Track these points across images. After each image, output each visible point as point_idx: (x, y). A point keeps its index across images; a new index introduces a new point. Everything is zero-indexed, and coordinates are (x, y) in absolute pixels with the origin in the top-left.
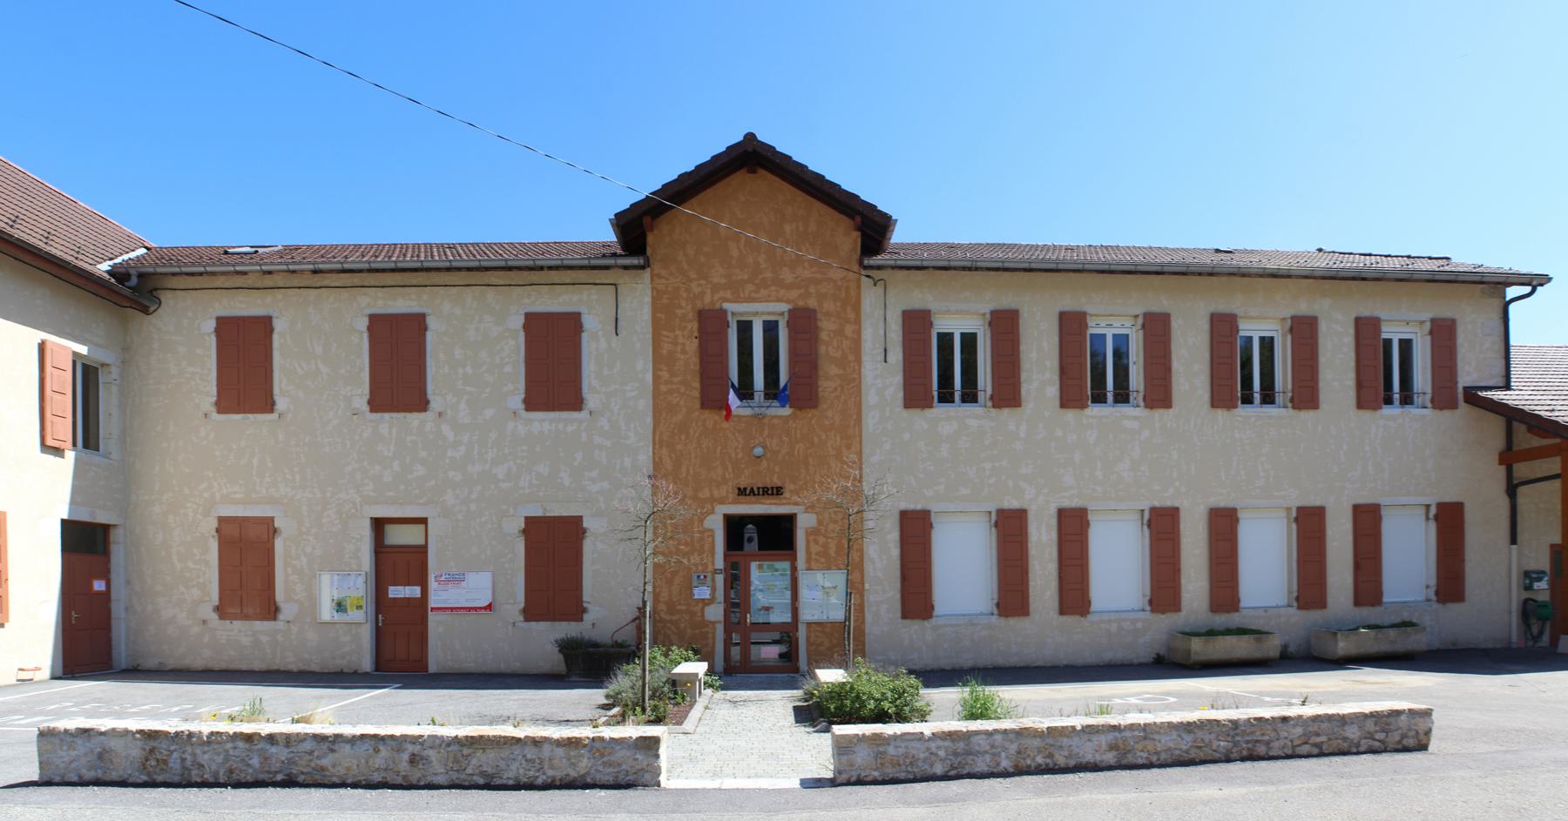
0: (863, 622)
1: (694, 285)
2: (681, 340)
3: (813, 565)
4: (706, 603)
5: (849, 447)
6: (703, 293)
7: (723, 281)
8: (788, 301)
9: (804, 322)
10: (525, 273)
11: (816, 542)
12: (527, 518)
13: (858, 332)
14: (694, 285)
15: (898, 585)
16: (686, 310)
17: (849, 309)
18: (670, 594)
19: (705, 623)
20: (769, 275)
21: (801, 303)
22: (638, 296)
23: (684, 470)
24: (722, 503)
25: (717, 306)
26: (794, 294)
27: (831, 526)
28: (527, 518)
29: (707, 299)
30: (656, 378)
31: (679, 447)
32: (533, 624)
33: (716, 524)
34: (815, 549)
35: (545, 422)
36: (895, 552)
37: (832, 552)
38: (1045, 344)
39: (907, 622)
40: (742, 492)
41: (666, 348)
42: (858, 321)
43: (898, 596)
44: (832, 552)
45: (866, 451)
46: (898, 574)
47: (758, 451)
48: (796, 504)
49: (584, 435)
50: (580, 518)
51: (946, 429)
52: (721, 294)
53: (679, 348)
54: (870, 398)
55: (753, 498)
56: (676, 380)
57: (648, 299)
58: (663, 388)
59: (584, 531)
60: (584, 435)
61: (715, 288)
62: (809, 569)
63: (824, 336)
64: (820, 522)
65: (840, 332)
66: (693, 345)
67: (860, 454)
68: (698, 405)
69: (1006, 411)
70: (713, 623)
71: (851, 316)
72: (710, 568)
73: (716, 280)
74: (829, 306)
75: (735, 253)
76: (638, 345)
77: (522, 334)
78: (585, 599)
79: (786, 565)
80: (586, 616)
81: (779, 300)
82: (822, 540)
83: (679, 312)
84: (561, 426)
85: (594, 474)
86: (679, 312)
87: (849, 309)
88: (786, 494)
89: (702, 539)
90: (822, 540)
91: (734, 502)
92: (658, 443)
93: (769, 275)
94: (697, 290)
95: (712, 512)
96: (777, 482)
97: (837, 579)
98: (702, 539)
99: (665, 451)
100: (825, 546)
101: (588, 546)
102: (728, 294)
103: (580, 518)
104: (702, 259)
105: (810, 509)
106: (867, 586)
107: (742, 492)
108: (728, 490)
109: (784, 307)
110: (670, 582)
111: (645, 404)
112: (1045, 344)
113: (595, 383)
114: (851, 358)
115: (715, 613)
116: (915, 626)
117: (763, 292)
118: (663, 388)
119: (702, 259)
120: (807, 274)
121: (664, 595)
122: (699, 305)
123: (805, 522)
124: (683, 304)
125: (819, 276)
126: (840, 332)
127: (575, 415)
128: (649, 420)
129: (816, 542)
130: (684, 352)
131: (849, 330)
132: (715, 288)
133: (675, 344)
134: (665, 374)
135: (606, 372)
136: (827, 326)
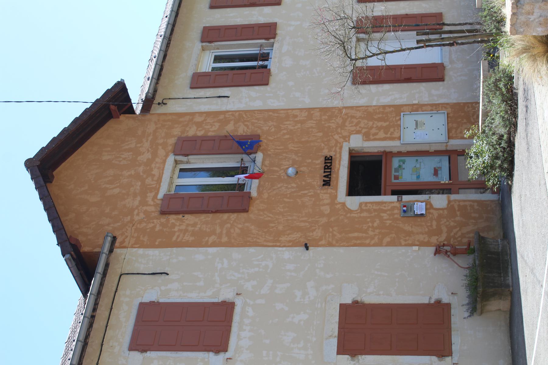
0: (447, 104)
1: (136, 218)
2: (183, 227)
3: (396, 135)
4: (429, 206)
5: (296, 116)
6: (145, 212)
7: (138, 198)
8: (167, 156)
9: (187, 146)
10: (89, 349)
11: (376, 134)
12: (339, 353)
13: (201, 114)
14: (136, 218)
15: (415, 84)
16: (158, 223)
17: (181, 120)
18: (422, 233)
19: (450, 206)
20: (141, 169)
21: (170, 148)
22: (136, 258)
23: (302, 224)
24: (336, 197)
25: (159, 202)
26: (161, 152)
27: (362, 125)
28: (339, 353)
29: (152, 209)
30: (214, 245)
31: (281, 228)
32: (454, 348)
33: (354, 202)
34: (382, 134)
35: (240, 335)
36: (386, 87)
37: (385, 124)
38: (231, 15)
39: (447, 78)
40: (327, 183)
41: (188, 238)
42: (193, 114)
43: (424, 84)
44: (385, 124)
45: (300, 106)
46: (405, 85)
47: (291, 171)
48: (341, 148)
49: (259, 301)
50: (341, 305)
51: (288, 62)
52: (149, 200)
53: (190, 228)
54: (257, 105)
55: (333, 176)
56: (218, 230)
57: (141, 251)
58: (225, 239)
59: (355, 302)
60: (259, 301)
61: (143, 203)
62: (399, 138)
63: (200, 133)
64: (358, 132)
65: (199, 125)
66: (190, 219)
67: (301, 110)
68: (244, 215)
69: (278, 32)
70: (449, 201)
71: (187, 118)
72: (397, 205)
73: (136, 203)
74: (177, 131)
75: (117, 191)
76: (181, 258)
77: (149, 354)
78: (426, 301)
79: (396, 162)
80: (445, 300)
81: (164, 162)
82: (374, 131)
83: (157, 229)
84: (246, 321)
85: (298, 293)
86: (157, 229)
87: (181, 120)
88: (332, 154)
89: (368, 211)
90: (374, 131)
91: (336, 189)
92: (276, 243)
93: (141, 169)
94: (142, 216)
95: (344, 204)
96: (320, 162)
97: (408, 120)
98: (368, 211)
99: (283, 239)
100: (379, 128)
101: (372, 297)
102: (150, 195)
103: (343, 307)
104: (116, 213)
105: (347, 138)
106: (416, 102)
107: (327, 183)
108: (325, 194)
109: (171, 159)
110: (409, 234)
111: (236, 253)
112: (231, 15)
113: (209, 293)
114: (222, 117)
115: (439, 201)
116: (450, 74)
117: (155, 172)
118: (225, 239)
119: (116, 213)
120: (147, 145)
121: (421, 237)
122: (156, 214)
123: (357, 142)
124: (151, 225)
125: (150, 138)
126: (199, 125)
127: (237, 310)
128: (252, 250)
129: (376, 134)
130: (194, 225)
131: (198, 119)
132: (143, 203)
133: (186, 231)
134: (212, 238)
135: (201, 283)
136: (192, 132)
